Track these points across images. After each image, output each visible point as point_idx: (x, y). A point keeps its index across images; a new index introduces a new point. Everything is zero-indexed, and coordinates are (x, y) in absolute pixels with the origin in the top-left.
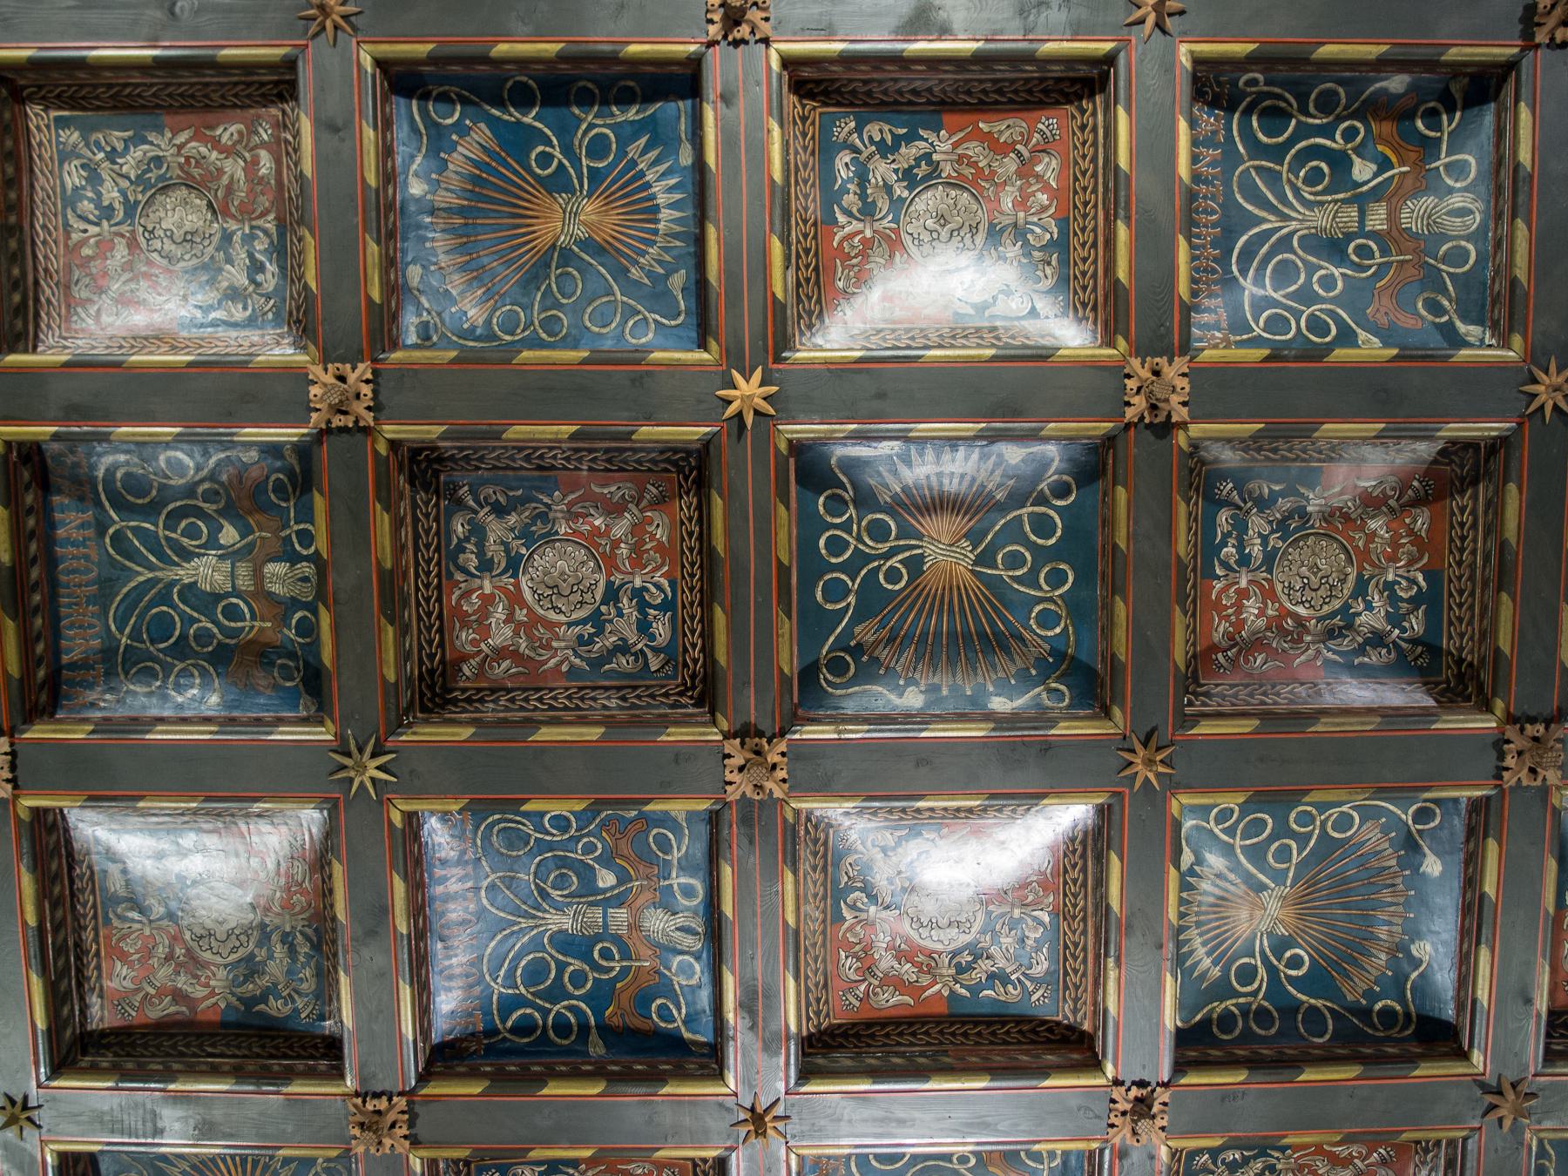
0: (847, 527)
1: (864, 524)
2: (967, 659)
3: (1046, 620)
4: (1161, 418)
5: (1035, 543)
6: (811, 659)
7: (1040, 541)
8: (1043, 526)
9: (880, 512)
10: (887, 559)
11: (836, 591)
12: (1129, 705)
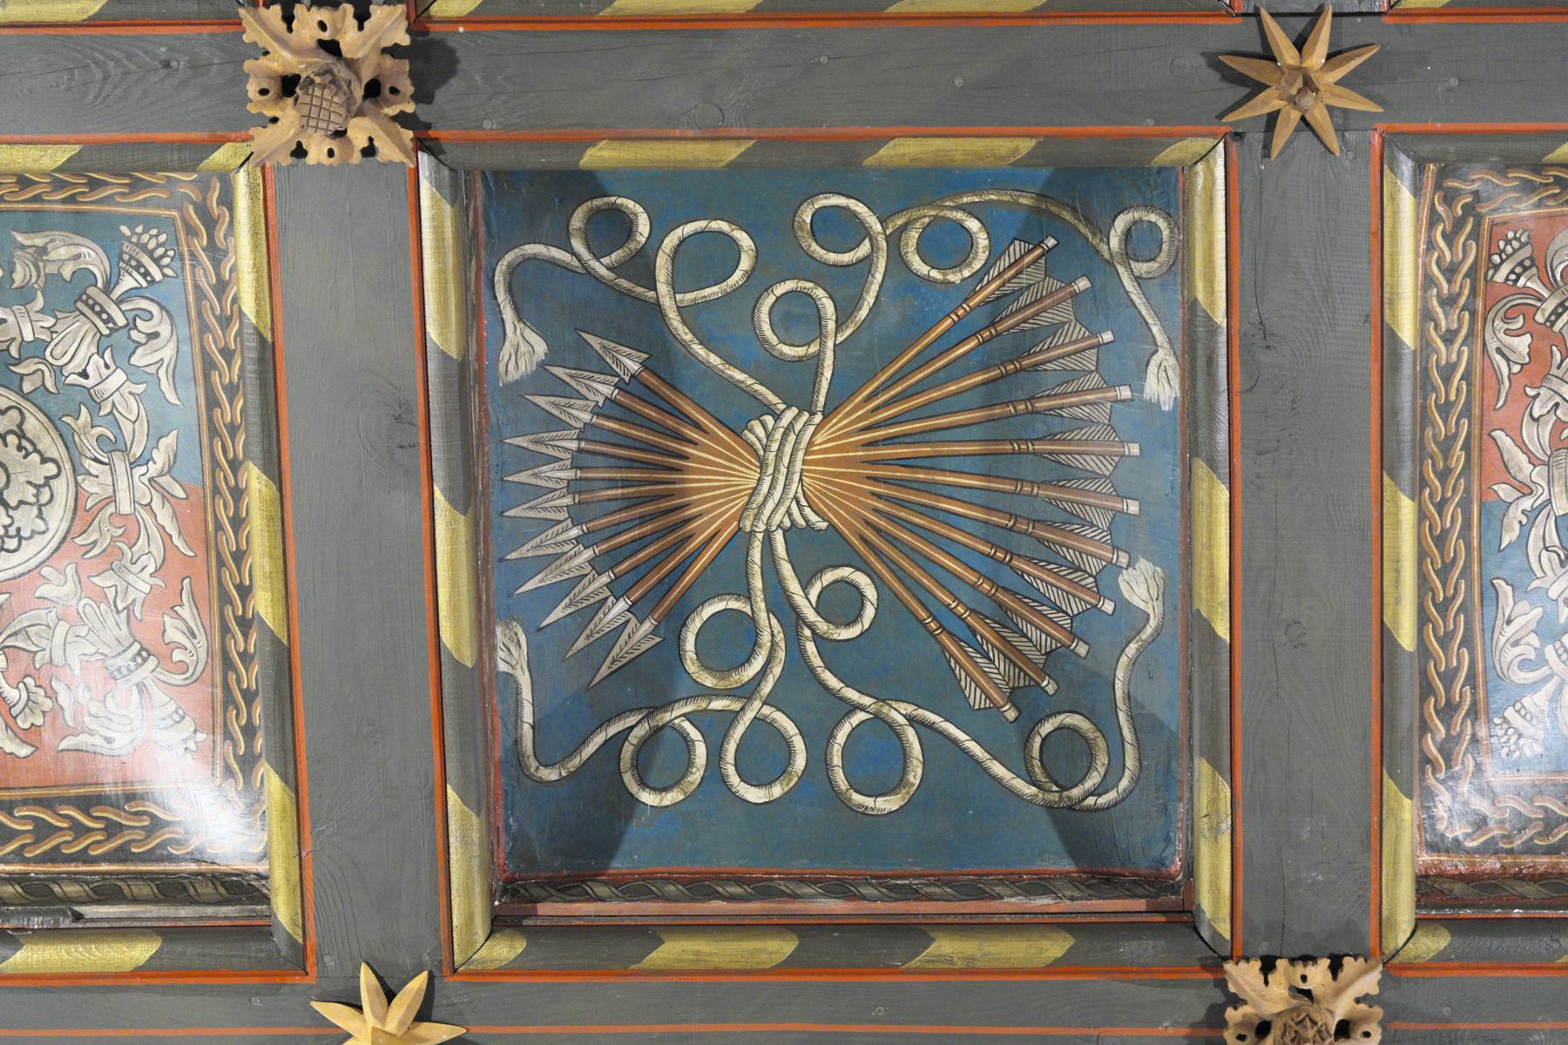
0: (716, 727)
1: (708, 681)
2: (1051, 437)
3: (946, 245)
4: (399, 74)
5: (750, 275)
6: (1045, 825)
7: (745, 263)
8: (704, 260)
9: (679, 640)
10: (800, 618)
11: (878, 758)
12: (1149, 126)
